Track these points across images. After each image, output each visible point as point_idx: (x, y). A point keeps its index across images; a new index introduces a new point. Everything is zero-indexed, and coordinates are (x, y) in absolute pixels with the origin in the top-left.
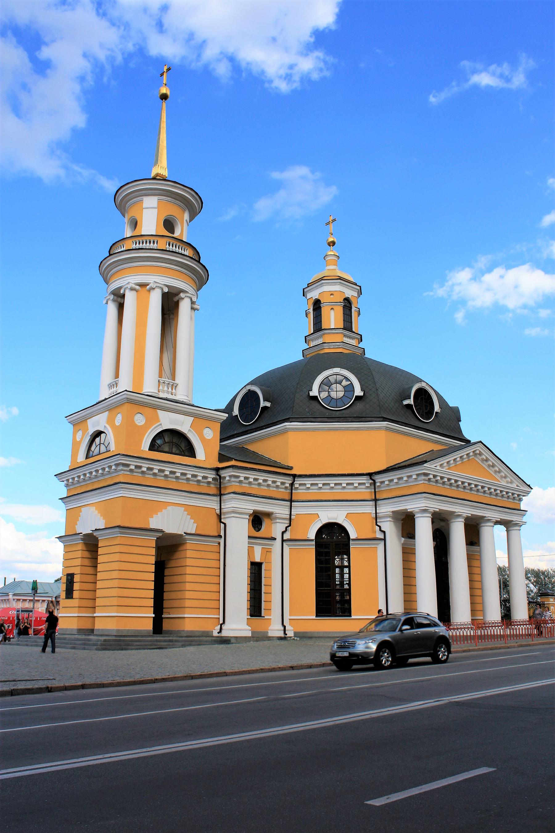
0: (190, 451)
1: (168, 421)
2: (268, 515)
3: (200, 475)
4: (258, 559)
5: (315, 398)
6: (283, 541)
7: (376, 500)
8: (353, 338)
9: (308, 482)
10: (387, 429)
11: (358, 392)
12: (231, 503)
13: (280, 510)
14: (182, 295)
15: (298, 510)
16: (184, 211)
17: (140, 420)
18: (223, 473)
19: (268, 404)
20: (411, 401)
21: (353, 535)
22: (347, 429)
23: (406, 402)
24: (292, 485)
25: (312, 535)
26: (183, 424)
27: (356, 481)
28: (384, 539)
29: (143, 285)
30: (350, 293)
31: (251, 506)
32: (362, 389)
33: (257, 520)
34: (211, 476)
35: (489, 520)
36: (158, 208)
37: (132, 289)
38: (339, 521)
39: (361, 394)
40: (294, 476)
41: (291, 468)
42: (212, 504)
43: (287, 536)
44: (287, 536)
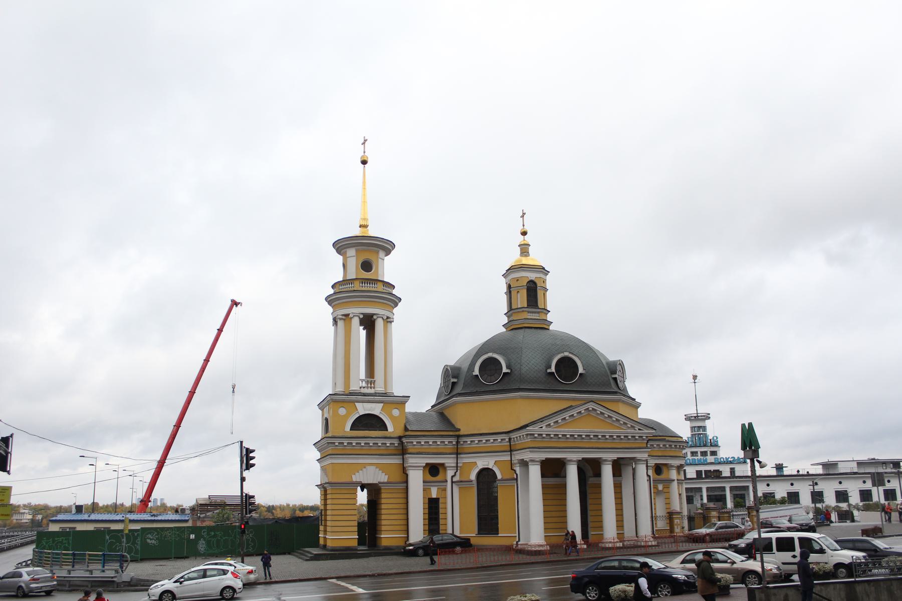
0: (383, 426)
1: (363, 409)
2: (443, 465)
3: (388, 443)
4: (434, 496)
5: (477, 376)
6: (452, 482)
7: (511, 451)
8: (538, 313)
9: (469, 440)
10: (522, 398)
11: (505, 370)
12: (411, 460)
13: (449, 461)
14: (375, 317)
15: (465, 459)
16: (378, 253)
17: (342, 411)
18: (404, 440)
19: (455, 380)
20: (553, 369)
21: (499, 476)
22: (487, 400)
23: (549, 371)
24: (458, 442)
25: (473, 476)
26: (375, 409)
27: (499, 438)
28: (517, 479)
29: (347, 315)
30: (532, 276)
31: (423, 461)
32: (507, 368)
33: (434, 470)
34: (396, 442)
35: (606, 460)
36: (357, 256)
37: (341, 319)
38: (490, 467)
39: (508, 371)
40: (458, 437)
41: (459, 430)
42: (397, 460)
43: (454, 480)
44: (454, 480)
